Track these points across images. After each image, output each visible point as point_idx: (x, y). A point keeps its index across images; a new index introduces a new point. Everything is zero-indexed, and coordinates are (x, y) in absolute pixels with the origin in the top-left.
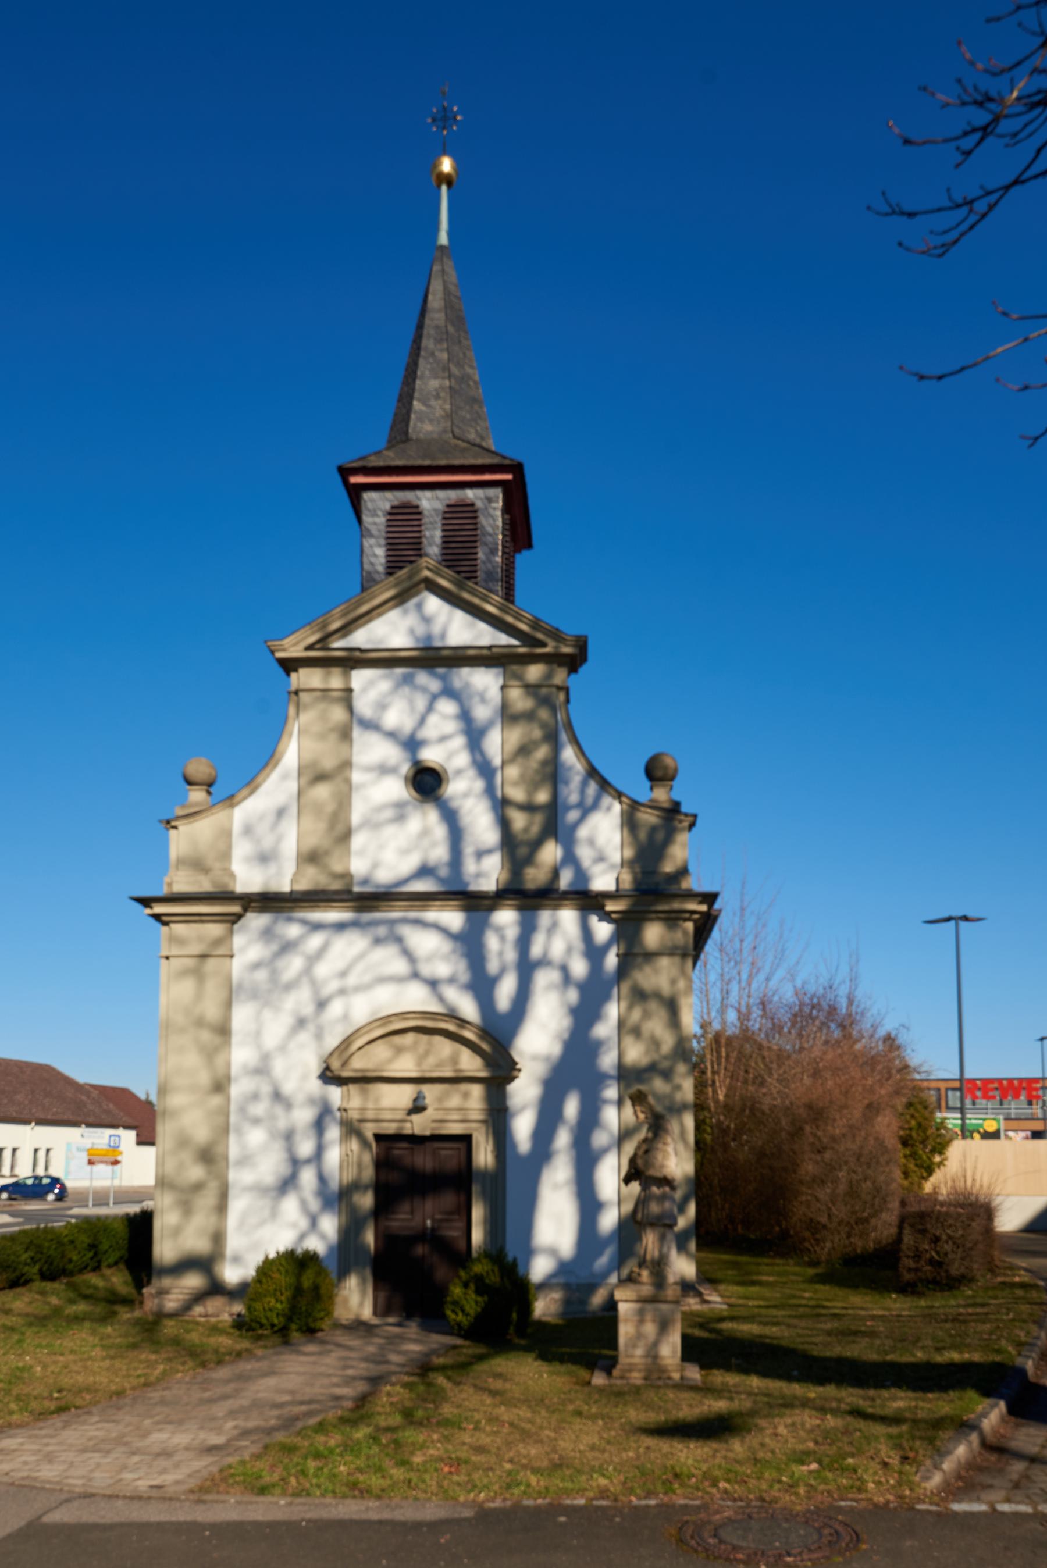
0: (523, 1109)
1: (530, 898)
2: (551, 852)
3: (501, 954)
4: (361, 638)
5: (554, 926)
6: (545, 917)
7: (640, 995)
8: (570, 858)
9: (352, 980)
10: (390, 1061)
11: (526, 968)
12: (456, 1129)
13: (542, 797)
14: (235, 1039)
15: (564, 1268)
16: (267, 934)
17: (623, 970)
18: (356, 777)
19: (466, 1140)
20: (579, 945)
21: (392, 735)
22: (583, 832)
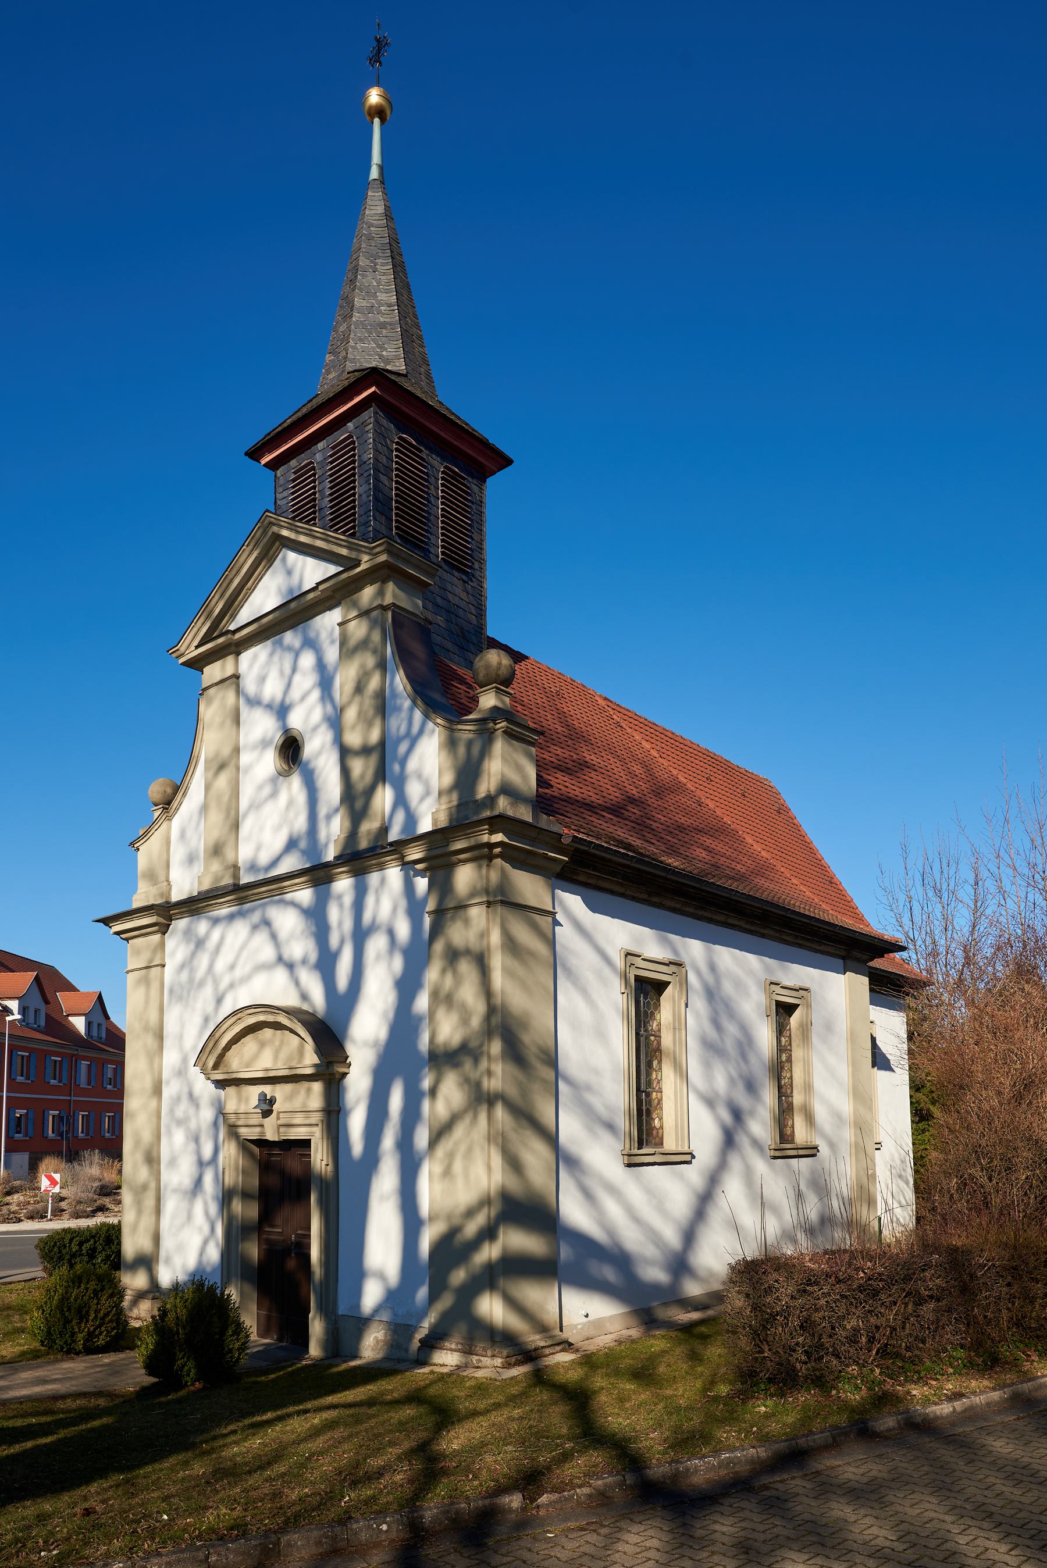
0: (358, 1101)
1: (359, 859)
2: (384, 798)
3: (340, 924)
4: (246, 614)
5: (383, 881)
6: (374, 878)
7: (453, 956)
8: (401, 800)
9: (238, 973)
10: (256, 1057)
11: (360, 935)
12: (298, 1133)
13: (375, 736)
14: (167, 1043)
15: (392, 1297)
16: (188, 933)
17: (436, 930)
18: (245, 758)
19: (306, 1144)
20: (403, 903)
21: (269, 706)
22: (412, 765)
